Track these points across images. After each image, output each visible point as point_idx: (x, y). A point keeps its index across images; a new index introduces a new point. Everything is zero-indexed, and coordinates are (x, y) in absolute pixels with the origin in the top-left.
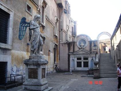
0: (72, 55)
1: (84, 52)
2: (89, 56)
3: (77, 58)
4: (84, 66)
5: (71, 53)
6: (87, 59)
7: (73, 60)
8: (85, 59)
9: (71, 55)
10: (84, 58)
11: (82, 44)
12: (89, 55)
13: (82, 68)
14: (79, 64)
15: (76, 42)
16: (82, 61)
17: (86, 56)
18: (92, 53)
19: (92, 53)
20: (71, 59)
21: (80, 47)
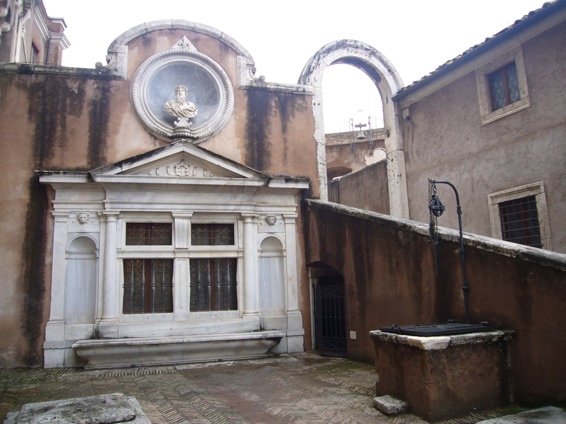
0: (75, 197)
1: (198, 176)
2: (245, 210)
3: (130, 226)
4: (202, 300)
5: (77, 171)
6: (222, 232)
7: (88, 245)
8: (205, 232)
9: (60, 197)
10: (194, 226)
11: (184, 103)
12: (240, 198)
13: (181, 324)
14: (147, 289)
15: (128, 84)
16: (182, 251)
17: (220, 207)
18: (272, 185)
19: (272, 185)
20: (62, 233)
21: (168, 131)
